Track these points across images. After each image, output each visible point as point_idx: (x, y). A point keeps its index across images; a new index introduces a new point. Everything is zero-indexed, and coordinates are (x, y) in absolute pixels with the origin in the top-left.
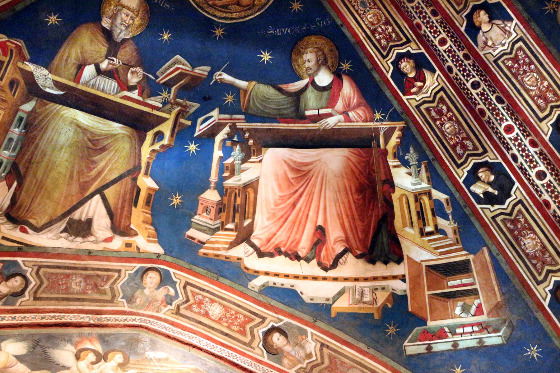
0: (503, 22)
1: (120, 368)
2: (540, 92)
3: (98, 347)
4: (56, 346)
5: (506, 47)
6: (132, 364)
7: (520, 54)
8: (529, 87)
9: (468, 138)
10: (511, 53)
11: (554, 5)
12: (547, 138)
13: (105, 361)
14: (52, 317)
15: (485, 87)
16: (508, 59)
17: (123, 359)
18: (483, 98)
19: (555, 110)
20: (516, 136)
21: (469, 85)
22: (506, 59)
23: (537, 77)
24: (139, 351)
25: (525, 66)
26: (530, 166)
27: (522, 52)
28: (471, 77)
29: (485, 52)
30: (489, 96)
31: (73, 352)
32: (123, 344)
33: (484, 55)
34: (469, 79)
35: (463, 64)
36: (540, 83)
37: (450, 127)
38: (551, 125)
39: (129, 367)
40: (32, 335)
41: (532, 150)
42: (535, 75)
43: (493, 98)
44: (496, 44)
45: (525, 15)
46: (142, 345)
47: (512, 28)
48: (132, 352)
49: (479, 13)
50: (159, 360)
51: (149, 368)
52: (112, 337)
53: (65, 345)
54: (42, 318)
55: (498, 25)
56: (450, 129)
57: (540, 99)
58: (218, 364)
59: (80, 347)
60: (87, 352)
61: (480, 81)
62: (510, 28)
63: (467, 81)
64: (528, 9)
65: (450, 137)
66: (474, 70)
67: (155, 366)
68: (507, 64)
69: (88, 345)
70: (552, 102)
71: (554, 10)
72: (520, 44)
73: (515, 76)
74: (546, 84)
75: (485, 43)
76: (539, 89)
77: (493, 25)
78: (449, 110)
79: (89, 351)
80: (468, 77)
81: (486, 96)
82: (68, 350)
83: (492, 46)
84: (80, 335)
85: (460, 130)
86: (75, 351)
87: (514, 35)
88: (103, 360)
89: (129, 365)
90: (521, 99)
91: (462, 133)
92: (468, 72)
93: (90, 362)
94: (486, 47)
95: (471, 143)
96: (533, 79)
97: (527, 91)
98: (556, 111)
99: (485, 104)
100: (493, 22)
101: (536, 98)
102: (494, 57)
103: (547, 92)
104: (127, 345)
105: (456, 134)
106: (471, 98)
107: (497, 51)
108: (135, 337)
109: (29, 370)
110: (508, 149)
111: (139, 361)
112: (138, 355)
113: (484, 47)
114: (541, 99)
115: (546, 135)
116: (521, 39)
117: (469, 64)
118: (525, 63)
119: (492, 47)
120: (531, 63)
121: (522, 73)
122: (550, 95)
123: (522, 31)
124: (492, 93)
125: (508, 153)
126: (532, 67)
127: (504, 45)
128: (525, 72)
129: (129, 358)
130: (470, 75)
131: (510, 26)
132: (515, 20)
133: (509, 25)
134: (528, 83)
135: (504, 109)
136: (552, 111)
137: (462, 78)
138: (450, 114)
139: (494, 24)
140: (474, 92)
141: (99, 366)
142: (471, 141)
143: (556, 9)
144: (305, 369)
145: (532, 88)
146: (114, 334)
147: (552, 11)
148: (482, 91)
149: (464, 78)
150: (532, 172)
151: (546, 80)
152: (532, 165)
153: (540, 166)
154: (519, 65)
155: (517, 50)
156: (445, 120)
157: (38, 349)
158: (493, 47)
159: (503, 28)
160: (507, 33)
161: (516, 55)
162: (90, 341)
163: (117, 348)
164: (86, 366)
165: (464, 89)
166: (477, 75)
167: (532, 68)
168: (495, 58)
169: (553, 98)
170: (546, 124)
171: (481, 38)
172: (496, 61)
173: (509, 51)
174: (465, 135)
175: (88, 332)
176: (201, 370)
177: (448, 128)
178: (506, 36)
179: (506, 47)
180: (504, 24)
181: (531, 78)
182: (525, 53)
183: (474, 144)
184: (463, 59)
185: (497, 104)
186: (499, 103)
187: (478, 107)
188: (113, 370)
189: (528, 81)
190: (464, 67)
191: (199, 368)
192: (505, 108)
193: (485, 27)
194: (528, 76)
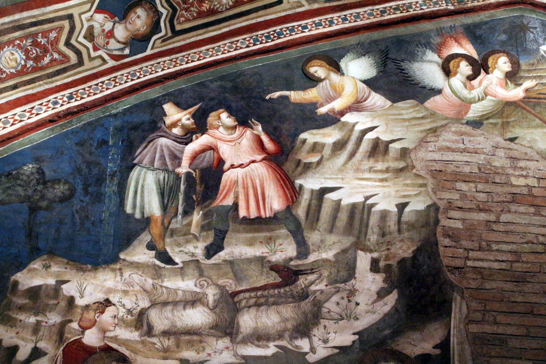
1: (510, 81)
3: (469, 49)
4: (413, 57)
13: (487, 73)
14: (395, 9)
17: (509, 64)
24: (532, 46)
31: (438, 63)
32: (503, 37)
39: (521, 78)
40: (376, 42)
46: (532, 35)
52: (484, 27)
53: (424, 53)
54: (383, 12)
59: (447, 53)
60: (457, 60)
69: (456, 49)
79: (460, 58)
82: (431, 62)
84: (440, 32)
86: (440, 61)
88: (482, 71)
89: (522, 74)
93: (465, 77)
104: (510, 38)
108: (518, 22)
109: (389, 103)
111: (534, 64)
112: (530, 54)
129: (518, 62)
141: (480, 83)
146: (486, 23)
157: (391, 66)
162: (456, 41)
163: (497, 47)
175: (449, 24)
188: (501, 86)
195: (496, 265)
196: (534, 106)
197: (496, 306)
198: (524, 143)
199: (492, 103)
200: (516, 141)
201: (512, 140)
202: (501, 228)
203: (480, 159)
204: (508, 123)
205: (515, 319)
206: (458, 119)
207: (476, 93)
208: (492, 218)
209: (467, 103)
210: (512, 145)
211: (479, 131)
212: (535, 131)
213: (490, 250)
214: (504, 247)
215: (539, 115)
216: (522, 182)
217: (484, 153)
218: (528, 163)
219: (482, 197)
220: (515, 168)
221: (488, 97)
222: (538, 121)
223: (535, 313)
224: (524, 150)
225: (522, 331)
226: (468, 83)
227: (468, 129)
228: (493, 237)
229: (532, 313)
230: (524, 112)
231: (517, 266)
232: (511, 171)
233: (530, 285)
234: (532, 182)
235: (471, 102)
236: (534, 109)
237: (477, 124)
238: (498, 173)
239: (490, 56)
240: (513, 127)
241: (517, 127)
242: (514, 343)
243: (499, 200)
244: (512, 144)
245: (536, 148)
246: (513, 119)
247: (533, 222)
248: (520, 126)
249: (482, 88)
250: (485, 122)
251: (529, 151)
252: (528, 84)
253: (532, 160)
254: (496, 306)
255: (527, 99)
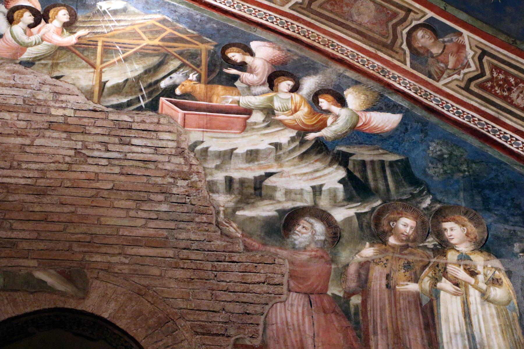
1: (66, 30)
6: (80, 22)
13: (47, 22)
31: (3, 13)
39: (76, 27)
48: (79, 4)
50: (115, 12)
51: (103, 24)
58: (191, 9)
60: (21, 11)
67: (111, 21)
79: (24, 9)
86: (6, 11)
88: (43, 20)
89: (78, 24)
93: (27, 25)
111: (89, 17)
112: (88, 8)
129: (76, 14)
144: (301, 4)
164: (22, 31)
176: (170, 19)
188: (58, 33)
191: (167, 18)
195: (22, 181)
196: (83, 51)
197: (15, 215)
198: (69, 80)
199: (46, 48)
200: (61, 79)
201: (58, 78)
202: (34, 150)
203: (27, 93)
204: (57, 64)
205: (30, 226)
206: (12, 60)
207: (33, 39)
208: (27, 141)
209: (24, 46)
210: (58, 82)
211: (29, 70)
212: (80, 71)
213: (19, 168)
214: (34, 166)
215: (86, 59)
216: (61, 112)
217: (31, 88)
218: (69, 97)
219: (22, 124)
220: (56, 101)
221: (44, 42)
222: (84, 63)
223: (48, 220)
224: (67, 86)
225: (34, 235)
226: (28, 30)
227: (21, 68)
228: (25, 157)
229: (45, 220)
230: (74, 55)
231: (42, 182)
232: (52, 104)
233: (49, 198)
234: (69, 112)
235: (27, 46)
236: (82, 53)
237: (29, 64)
238: (41, 105)
239: (51, 8)
240: (62, 67)
241: (65, 68)
242: (25, 245)
243: (37, 127)
244: (58, 81)
245: (78, 84)
246: (61, 61)
247: (63, 145)
248: (67, 67)
249: (40, 34)
250: (37, 63)
251: (71, 87)
252: (81, 33)
253: (73, 95)
254: (15, 215)
255: (77, 45)
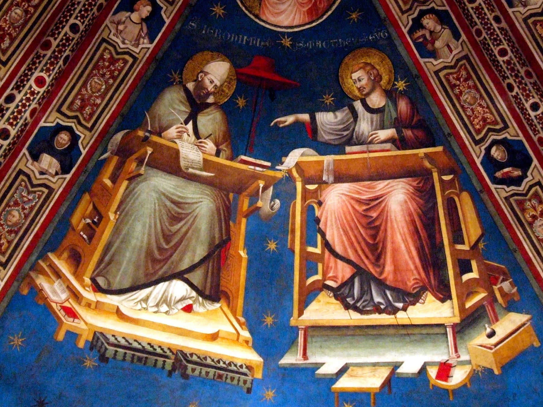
0: (146, 34)
2: (88, 99)
5: (122, 46)
7: (120, 64)
8: (89, 86)
9: (12, 40)
10: (118, 53)
11: (178, 80)
12: (42, 124)
15: (76, 39)
16: (110, 53)
18: (64, 41)
19: (75, 120)
20: (36, 92)
21: (72, 21)
22: (110, 51)
23: (102, 90)
25: (109, 73)
26: (9, 119)
27: (123, 65)
28: (82, 21)
29: (109, 25)
30: (68, 47)
33: (107, 25)
34: (79, 18)
35: (93, 7)
36: (97, 95)
37: (19, 15)
38: (58, 123)
41: (27, 114)
42: (104, 87)
43: (67, 53)
44: (122, 35)
45: (160, 54)
47: (144, 46)
49: (148, 5)
55: (142, 29)
56: (16, 16)
57: (80, 101)
61: (80, 33)
62: (143, 43)
63: (76, 18)
64: (167, 54)
65: (8, 18)
66: (89, 21)
68: (105, 54)
70: (82, 114)
71: (174, 81)
72: (131, 60)
73: (96, 67)
74: (98, 101)
75: (119, 23)
76: (91, 96)
77: (140, 25)
78: (36, 7)
80: (80, 16)
81: (67, 44)
83: (119, 31)
85: (18, 28)
87: (137, 50)
90: (74, 81)
91: (15, 31)
92: (86, 15)
94: (116, 25)
95: (8, 45)
96: (99, 87)
97: (84, 85)
98: (74, 123)
99: (58, 46)
100: (144, 25)
101: (79, 97)
102: (108, 37)
103: (90, 105)
105: (12, 24)
106: (58, 28)
107: (114, 38)
110: (18, 88)
113: (115, 23)
114: (81, 103)
115: (45, 122)
116: (135, 59)
117: (94, 13)
118: (112, 72)
119: (117, 32)
120: (115, 78)
121: (101, 72)
122: (88, 110)
123: (143, 58)
124: (71, 49)
125: (12, 89)
126: (111, 81)
127: (124, 43)
128: (103, 75)
130: (83, 19)
131: (145, 43)
132: (152, 46)
133: (145, 41)
134: (93, 83)
135: (59, 68)
136: (73, 119)
137: (77, 11)
138: (32, 10)
139: (142, 26)
140: (67, 29)
142: (11, 44)
143: (175, 84)
145: (89, 88)
147: (172, 80)
148: (71, 38)
149: (78, 13)
150: (4, 123)
151: (102, 101)
152: (11, 121)
153: (14, 129)
154: (109, 67)
155: (123, 59)
156: (24, 6)
158: (119, 32)
159: (141, 35)
160: (137, 42)
161: (118, 60)
165: (65, 17)
166: (86, 26)
167: (109, 81)
168: (106, 38)
169: (87, 114)
170: (57, 118)
171: (123, 15)
172: (104, 40)
173: (120, 50)
174: (14, 34)
177: (16, 13)
178: (133, 43)
179: (122, 46)
180: (145, 36)
181: (99, 84)
182: (123, 68)
183: (8, 48)
184: (98, 4)
185: (63, 58)
186: (63, 61)
187: (52, 39)
189: (95, 82)
190: (90, 9)
192: (60, 69)
193: (135, 16)
194: (100, 80)
